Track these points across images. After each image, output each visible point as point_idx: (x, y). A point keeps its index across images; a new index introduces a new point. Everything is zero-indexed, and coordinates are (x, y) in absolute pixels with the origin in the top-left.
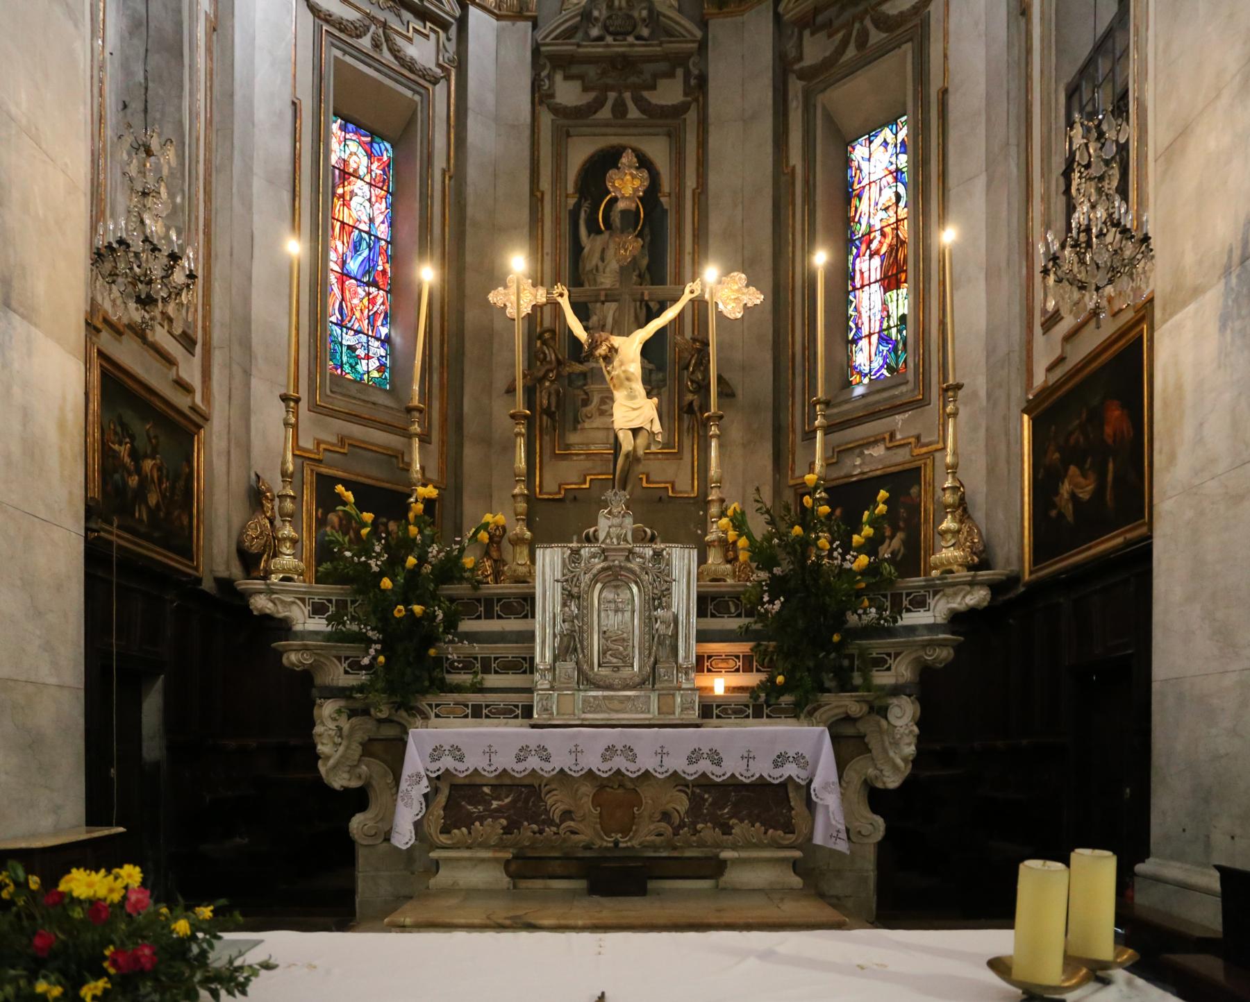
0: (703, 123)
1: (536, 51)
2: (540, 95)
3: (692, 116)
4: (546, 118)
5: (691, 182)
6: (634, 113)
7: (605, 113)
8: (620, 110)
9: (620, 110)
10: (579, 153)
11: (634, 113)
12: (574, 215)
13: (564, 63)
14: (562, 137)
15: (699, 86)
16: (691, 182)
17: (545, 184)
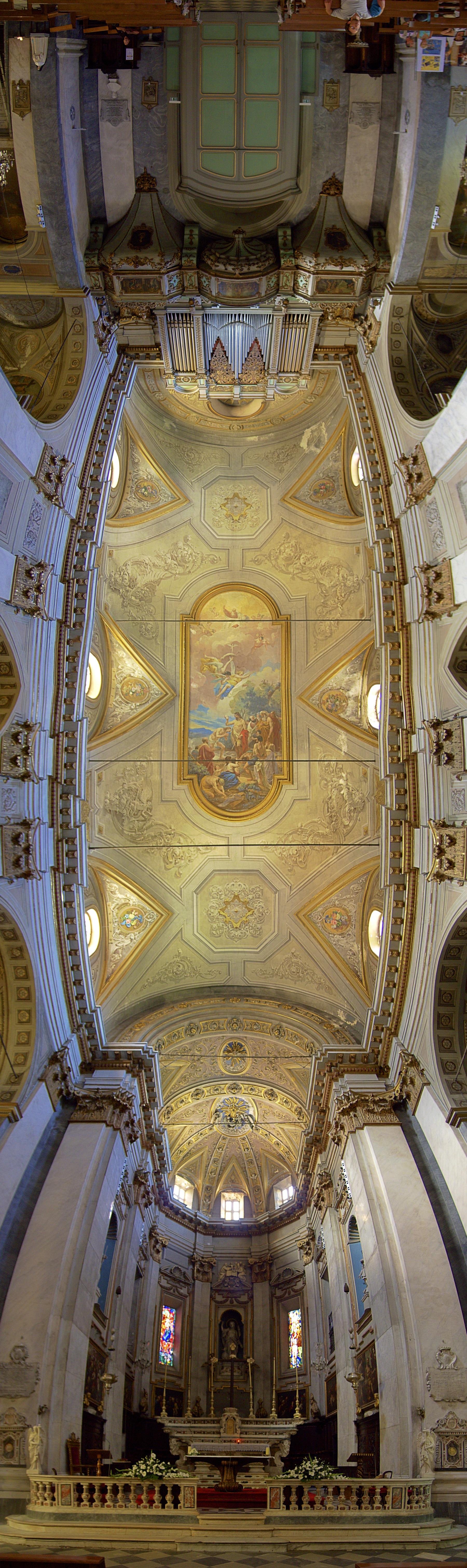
0: (252, 1305)
1: (211, 1288)
2: (212, 1298)
3: (250, 1304)
4: (213, 1303)
5: (249, 1318)
6: (235, 1303)
7: (228, 1303)
8: (232, 1302)
9: (232, 1302)
10: (222, 1311)
11: (235, 1303)
12: (220, 1325)
13: (218, 1291)
14: (217, 1308)
15: (251, 1298)
16: (249, 1318)
17: (213, 1318)
